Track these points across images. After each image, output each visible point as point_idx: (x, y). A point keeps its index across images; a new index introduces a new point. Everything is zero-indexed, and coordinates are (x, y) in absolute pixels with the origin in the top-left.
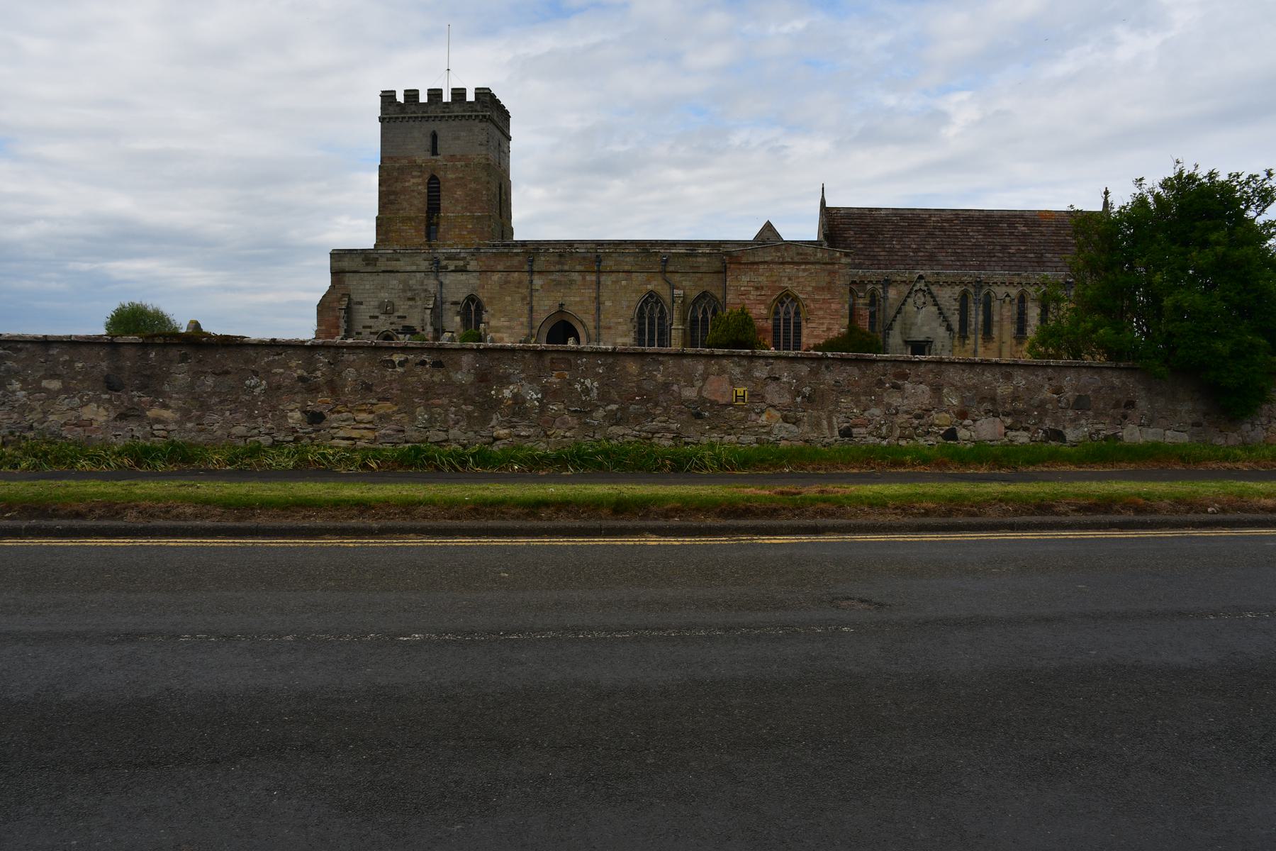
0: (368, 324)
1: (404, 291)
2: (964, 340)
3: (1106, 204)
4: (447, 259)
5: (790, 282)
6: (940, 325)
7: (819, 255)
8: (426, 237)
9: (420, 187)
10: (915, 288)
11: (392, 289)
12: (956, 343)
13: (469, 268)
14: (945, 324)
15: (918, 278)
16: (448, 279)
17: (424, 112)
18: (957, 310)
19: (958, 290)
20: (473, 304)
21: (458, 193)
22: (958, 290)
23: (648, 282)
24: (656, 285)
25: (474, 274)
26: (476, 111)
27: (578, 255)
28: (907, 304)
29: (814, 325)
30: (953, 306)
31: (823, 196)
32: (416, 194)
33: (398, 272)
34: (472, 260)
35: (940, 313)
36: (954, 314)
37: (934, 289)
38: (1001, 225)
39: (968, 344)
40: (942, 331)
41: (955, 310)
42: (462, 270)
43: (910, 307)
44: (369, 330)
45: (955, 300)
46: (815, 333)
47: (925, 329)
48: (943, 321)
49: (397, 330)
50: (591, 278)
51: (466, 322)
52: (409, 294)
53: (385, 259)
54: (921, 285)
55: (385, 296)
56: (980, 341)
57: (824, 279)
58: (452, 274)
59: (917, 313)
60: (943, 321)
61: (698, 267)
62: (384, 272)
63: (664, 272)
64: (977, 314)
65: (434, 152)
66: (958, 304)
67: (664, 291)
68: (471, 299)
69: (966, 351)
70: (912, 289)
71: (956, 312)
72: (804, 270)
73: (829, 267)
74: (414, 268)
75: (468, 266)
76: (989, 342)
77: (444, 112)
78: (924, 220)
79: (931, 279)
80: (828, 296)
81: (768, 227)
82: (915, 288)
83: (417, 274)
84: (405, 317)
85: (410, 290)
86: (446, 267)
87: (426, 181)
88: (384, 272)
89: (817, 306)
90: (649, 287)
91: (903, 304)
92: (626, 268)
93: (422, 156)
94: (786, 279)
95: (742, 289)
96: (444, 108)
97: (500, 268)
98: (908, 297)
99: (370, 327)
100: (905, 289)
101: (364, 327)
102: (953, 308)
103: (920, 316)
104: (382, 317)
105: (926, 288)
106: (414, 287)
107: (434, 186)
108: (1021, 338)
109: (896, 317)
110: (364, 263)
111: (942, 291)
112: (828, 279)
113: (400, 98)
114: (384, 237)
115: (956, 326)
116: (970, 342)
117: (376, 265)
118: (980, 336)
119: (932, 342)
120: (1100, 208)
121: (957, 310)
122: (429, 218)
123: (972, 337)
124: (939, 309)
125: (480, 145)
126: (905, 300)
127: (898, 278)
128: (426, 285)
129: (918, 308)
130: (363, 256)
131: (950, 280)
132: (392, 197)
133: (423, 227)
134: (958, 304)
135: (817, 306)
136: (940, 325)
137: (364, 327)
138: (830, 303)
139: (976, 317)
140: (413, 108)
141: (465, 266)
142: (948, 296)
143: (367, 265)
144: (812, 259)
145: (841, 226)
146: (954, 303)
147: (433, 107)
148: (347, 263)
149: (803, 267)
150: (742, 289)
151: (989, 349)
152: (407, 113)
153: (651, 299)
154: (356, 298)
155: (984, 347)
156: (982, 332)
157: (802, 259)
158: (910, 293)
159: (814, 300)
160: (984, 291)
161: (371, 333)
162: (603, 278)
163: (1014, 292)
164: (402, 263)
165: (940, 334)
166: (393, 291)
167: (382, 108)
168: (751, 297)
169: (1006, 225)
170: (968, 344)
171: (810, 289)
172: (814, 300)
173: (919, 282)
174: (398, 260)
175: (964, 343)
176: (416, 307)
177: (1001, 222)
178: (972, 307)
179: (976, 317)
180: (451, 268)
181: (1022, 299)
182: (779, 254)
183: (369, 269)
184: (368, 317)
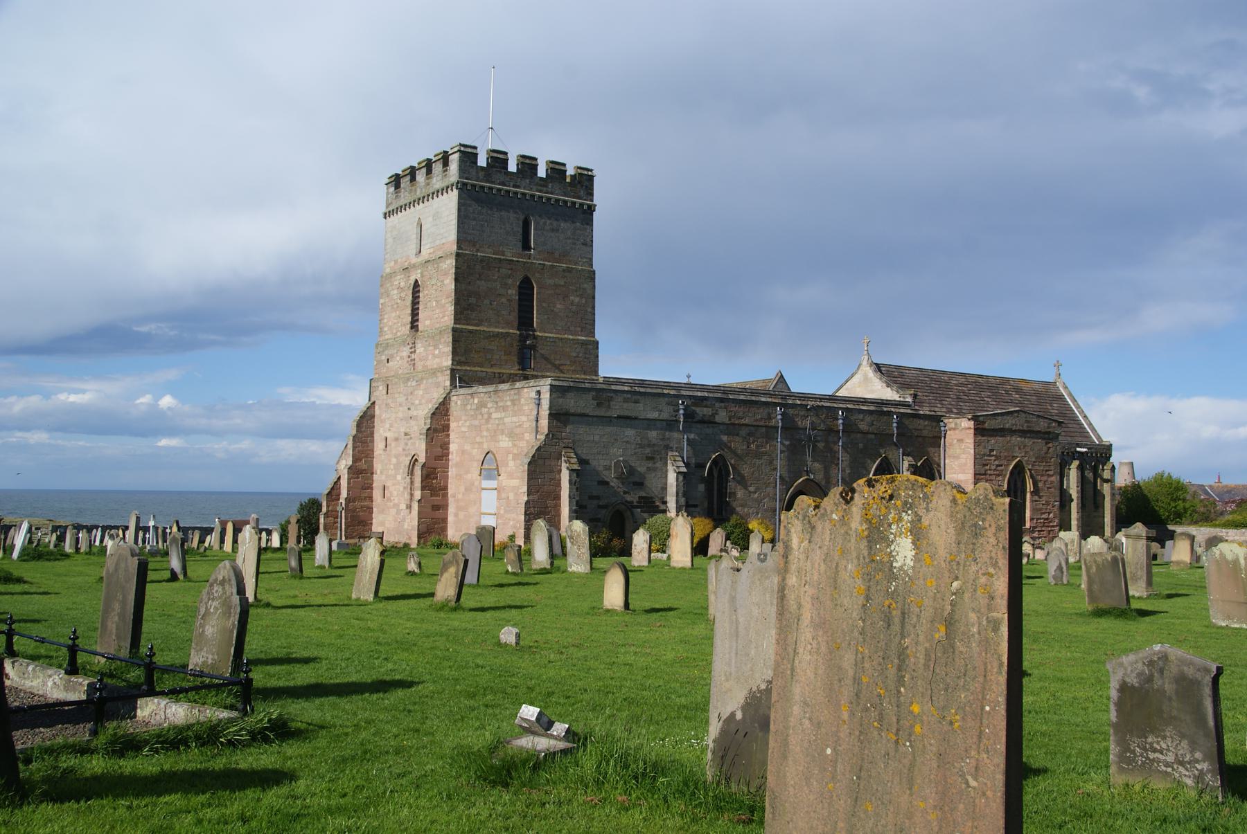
0: (595, 493)
1: (641, 446)
8: (519, 364)
9: (510, 292)
11: (627, 442)
13: (718, 419)
20: (716, 467)
21: (558, 306)
25: (721, 427)
32: (504, 300)
34: (721, 408)
44: (595, 502)
49: (632, 502)
51: (709, 490)
52: (648, 450)
53: (620, 399)
58: (699, 426)
61: (921, 430)
65: (526, 246)
74: (655, 415)
75: (717, 417)
77: (540, 191)
78: (947, 383)
81: (781, 379)
83: (658, 422)
85: (649, 445)
87: (518, 283)
96: (541, 186)
99: (598, 498)
101: (591, 498)
106: (654, 441)
107: (526, 288)
110: (595, 402)
113: (482, 161)
114: (463, 359)
117: (609, 407)
122: (523, 338)
125: (583, 244)
128: (668, 439)
132: (473, 300)
133: (515, 349)
137: (591, 498)
140: (502, 178)
141: (713, 415)
143: (599, 405)
147: (528, 181)
148: (572, 401)
152: (493, 183)
161: (600, 507)
164: (641, 406)
166: (628, 446)
174: (637, 402)
176: (655, 469)
184: (596, 483)
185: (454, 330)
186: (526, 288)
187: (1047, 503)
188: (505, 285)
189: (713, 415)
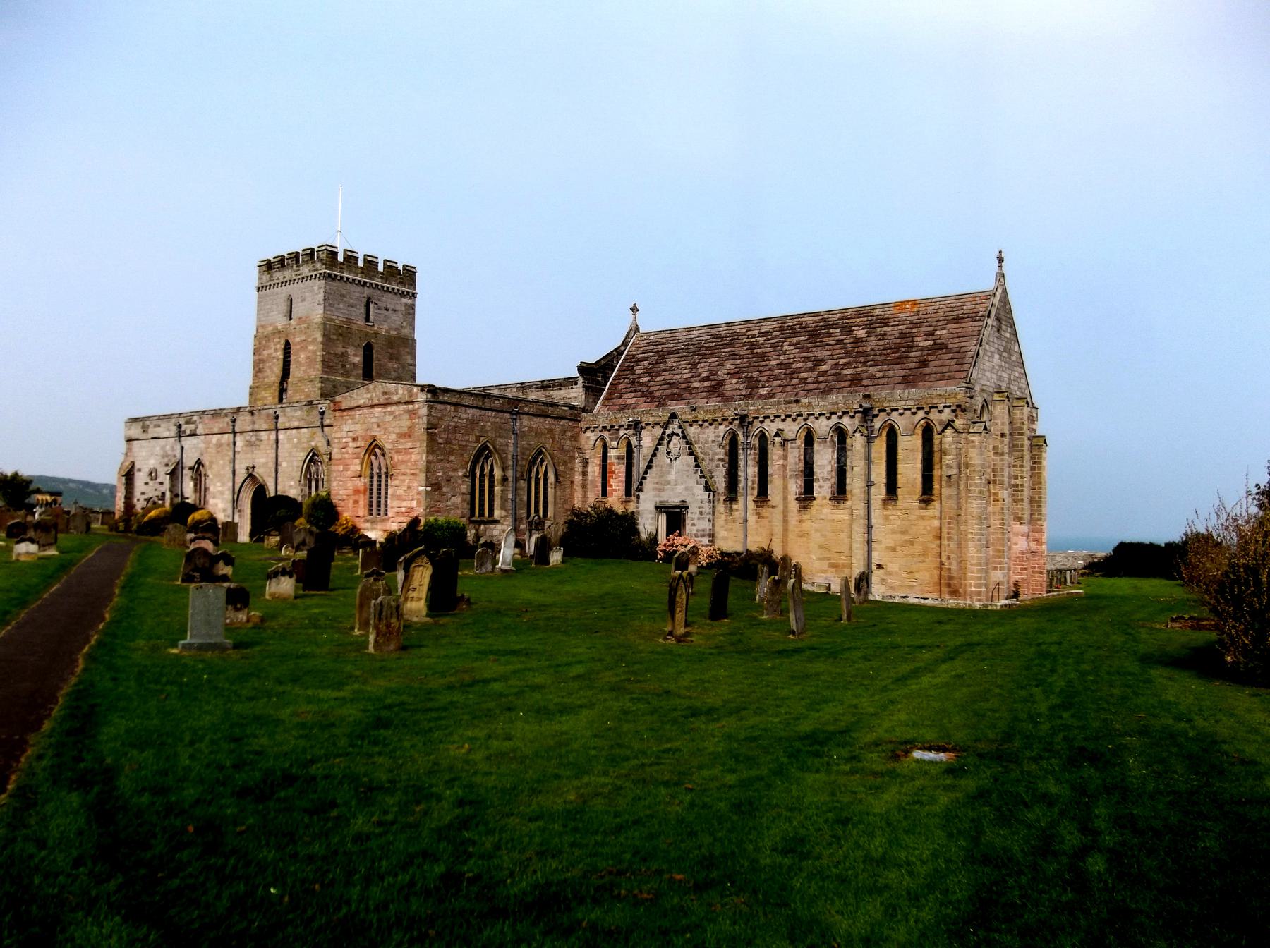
2: (731, 504)
3: (1000, 276)
4: (187, 423)
5: (378, 429)
6: (697, 484)
7: (400, 392)
10: (668, 432)
12: (721, 507)
14: (703, 480)
15: (670, 418)
16: (188, 442)
17: (284, 277)
18: (722, 460)
19: (722, 429)
22: (722, 429)
23: (312, 438)
24: (319, 442)
26: (317, 270)
27: (264, 412)
28: (658, 454)
29: (396, 483)
30: (717, 454)
31: (635, 320)
33: (159, 438)
35: (697, 466)
36: (718, 466)
37: (692, 431)
38: (831, 331)
39: (737, 510)
40: (701, 494)
41: (719, 460)
42: (193, 434)
43: (662, 457)
45: (720, 445)
46: (398, 494)
47: (680, 488)
48: (701, 477)
50: (273, 435)
52: (166, 460)
54: (674, 427)
55: (152, 463)
56: (751, 505)
57: (405, 423)
59: (670, 466)
60: (701, 477)
62: (153, 438)
63: (322, 426)
64: (746, 465)
66: (723, 451)
67: (322, 447)
68: (199, 463)
69: (734, 521)
70: (664, 433)
71: (721, 463)
72: (391, 413)
73: (410, 406)
74: (167, 434)
76: (763, 506)
79: (688, 417)
80: (409, 445)
82: (668, 432)
84: (161, 483)
86: (184, 432)
88: (153, 438)
89: (400, 458)
90: (313, 444)
91: (654, 455)
92: (296, 424)
93: (281, 322)
94: (375, 426)
95: (344, 440)
97: (216, 430)
98: (659, 444)
99: (143, 494)
100: (658, 431)
102: (717, 457)
103: (673, 473)
104: (151, 483)
105: (679, 431)
107: (287, 347)
108: (805, 500)
109: (646, 473)
111: (704, 433)
112: (409, 423)
115: (720, 483)
116: (739, 506)
118: (750, 498)
119: (687, 507)
120: (988, 284)
121: (722, 460)
122: (281, 384)
123: (741, 499)
124: (696, 460)
126: (656, 449)
127: (651, 420)
129: (671, 460)
130: (141, 423)
131: (709, 417)
132: (261, 366)
133: (277, 394)
134: (723, 451)
135: (400, 458)
136: (697, 484)
138: (411, 453)
139: (748, 470)
141: (195, 430)
142: (710, 439)
144: (395, 398)
145: (641, 355)
146: (718, 450)
149: (389, 409)
150: (344, 440)
151: (763, 518)
153: (313, 457)
154: (137, 466)
155: (758, 514)
156: (755, 492)
157: (387, 399)
158: (662, 439)
159: (398, 451)
160: (756, 428)
162: (281, 435)
163: (791, 429)
165: (696, 496)
167: (260, 279)
168: (350, 450)
169: (839, 330)
170: (737, 510)
171: (394, 437)
172: (398, 451)
173: (672, 423)
175: (731, 510)
177: (833, 326)
178: (741, 456)
179: (748, 470)
180: (188, 432)
181: (809, 440)
182: (369, 396)
183: (144, 436)
185: (251, 388)
186: (287, 347)
187: (409, 487)
188: (276, 350)
189: (195, 430)
